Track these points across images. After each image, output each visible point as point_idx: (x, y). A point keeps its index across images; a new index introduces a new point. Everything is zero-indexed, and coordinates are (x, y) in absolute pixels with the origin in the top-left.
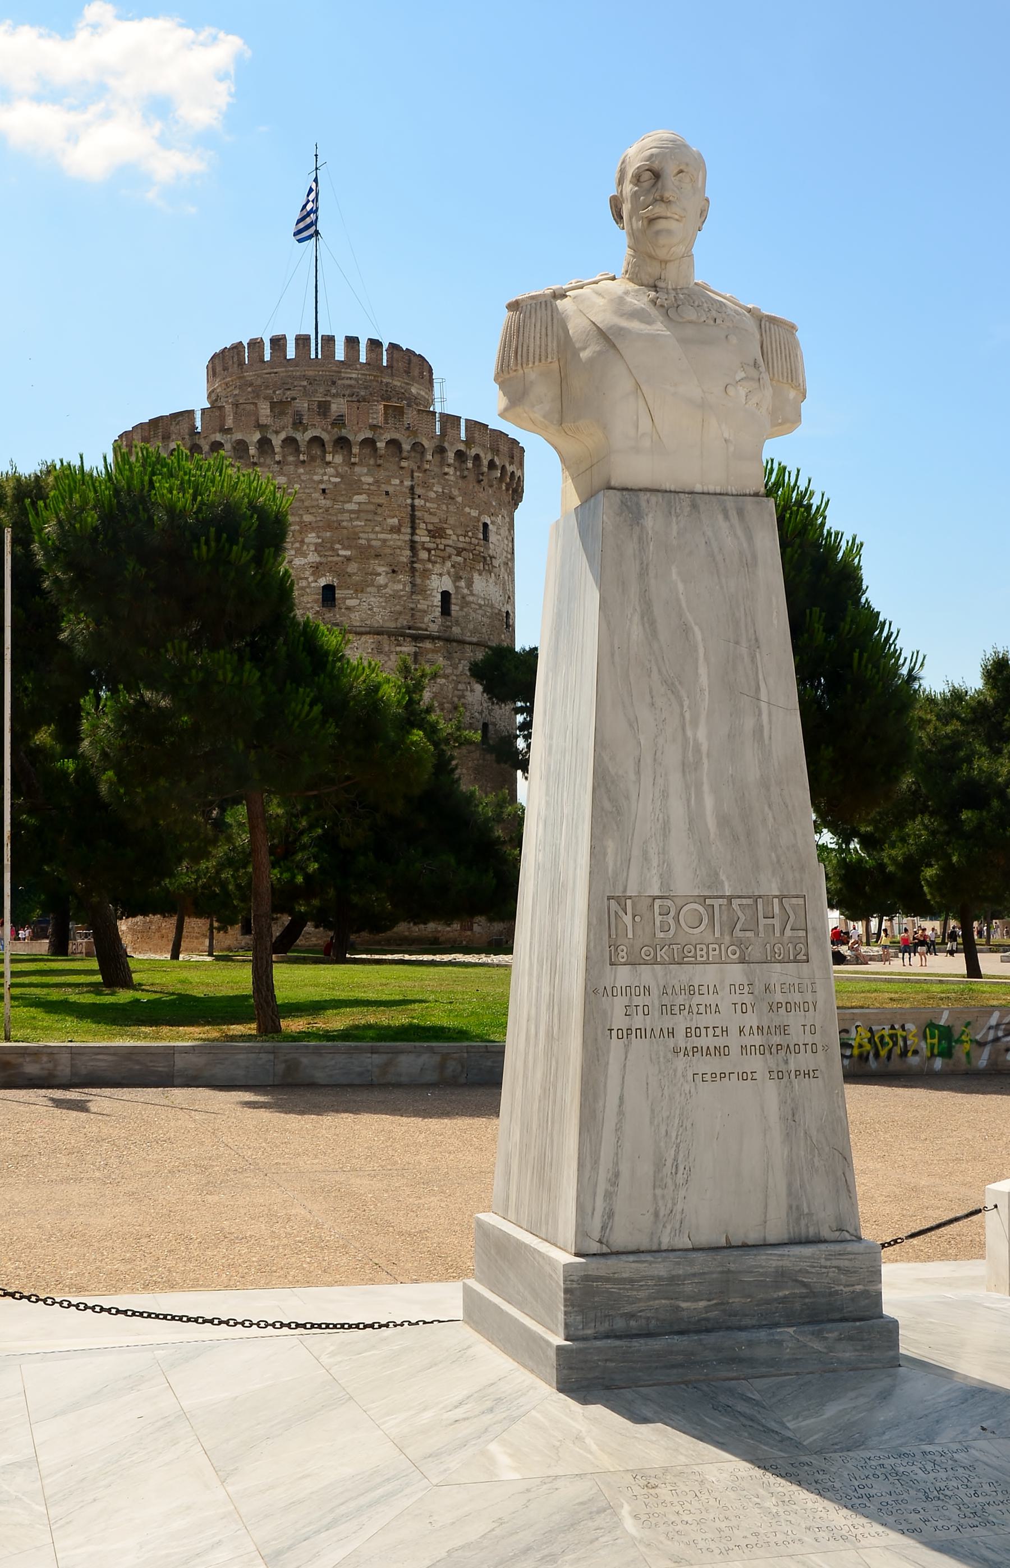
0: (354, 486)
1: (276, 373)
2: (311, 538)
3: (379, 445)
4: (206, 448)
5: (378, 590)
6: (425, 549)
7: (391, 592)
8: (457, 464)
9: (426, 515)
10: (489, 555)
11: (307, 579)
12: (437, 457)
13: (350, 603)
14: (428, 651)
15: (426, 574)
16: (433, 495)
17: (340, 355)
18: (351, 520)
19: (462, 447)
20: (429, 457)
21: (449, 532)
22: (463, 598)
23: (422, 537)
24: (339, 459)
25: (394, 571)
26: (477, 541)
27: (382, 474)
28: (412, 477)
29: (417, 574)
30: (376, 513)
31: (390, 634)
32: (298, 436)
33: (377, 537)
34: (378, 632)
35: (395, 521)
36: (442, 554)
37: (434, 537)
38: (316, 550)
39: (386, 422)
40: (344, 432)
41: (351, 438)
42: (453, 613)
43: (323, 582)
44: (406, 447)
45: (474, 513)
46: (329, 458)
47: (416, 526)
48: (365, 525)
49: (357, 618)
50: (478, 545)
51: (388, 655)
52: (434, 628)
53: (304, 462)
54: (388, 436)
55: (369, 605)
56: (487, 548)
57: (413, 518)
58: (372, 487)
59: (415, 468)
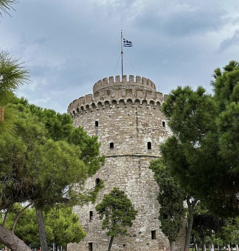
0: (119, 114)
1: (105, 88)
2: (107, 130)
3: (125, 101)
4: (80, 109)
5: (126, 143)
6: (142, 130)
7: (130, 143)
8: (152, 105)
9: (142, 120)
10: (166, 131)
11: (105, 141)
12: (144, 103)
13: (118, 147)
14: (143, 160)
15: (142, 137)
16: (144, 114)
17: (121, 81)
18: (118, 123)
19: (153, 100)
20: (141, 103)
21: (149, 124)
22: (156, 144)
24: (114, 107)
25: (131, 137)
26: (160, 127)
27: (127, 109)
28: (137, 110)
29: (139, 137)
30: (125, 121)
32: (101, 101)
33: (126, 127)
34: (126, 156)
36: (147, 131)
37: (144, 126)
38: (108, 133)
39: (127, 94)
40: (114, 99)
41: (116, 100)
42: (152, 148)
43: (110, 142)
44: (133, 101)
45: (159, 119)
46: (111, 106)
47: (138, 123)
48: (122, 124)
49: (120, 152)
50: (161, 128)
52: (145, 154)
53: (104, 109)
54: (127, 98)
55: (124, 147)
56: (165, 129)
57: (137, 121)
58: (124, 114)
59: (137, 107)
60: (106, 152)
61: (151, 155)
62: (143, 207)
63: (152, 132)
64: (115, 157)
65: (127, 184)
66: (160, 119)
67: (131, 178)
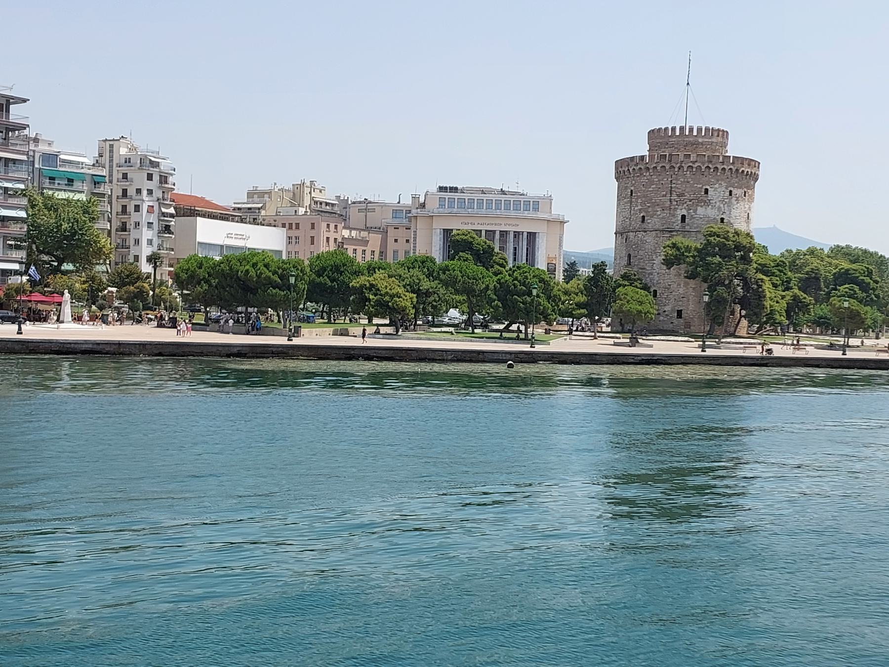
0: (652, 183)
2: (639, 201)
9: (676, 189)
13: (649, 221)
15: (675, 209)
19: (691, 164)
20: (676, 170)
22: (692, 216)
23: (674, 197)
27: (661, 178)
31: (660, 231)
32: (635, 168)
35: (664, 193)
43: (642, 215)
44: (667, 168)
46: (644, 174)
51: (660, 237)
52: (677, 228)
54: (661, 165)
57: (671, 191)
60: (638, 226)
61: (684, 230)
62: (670, 285)
63: (688, 203)
64: (646, 232)
65: (654, 262)
66: (701, 186)
67: (660, 255)
